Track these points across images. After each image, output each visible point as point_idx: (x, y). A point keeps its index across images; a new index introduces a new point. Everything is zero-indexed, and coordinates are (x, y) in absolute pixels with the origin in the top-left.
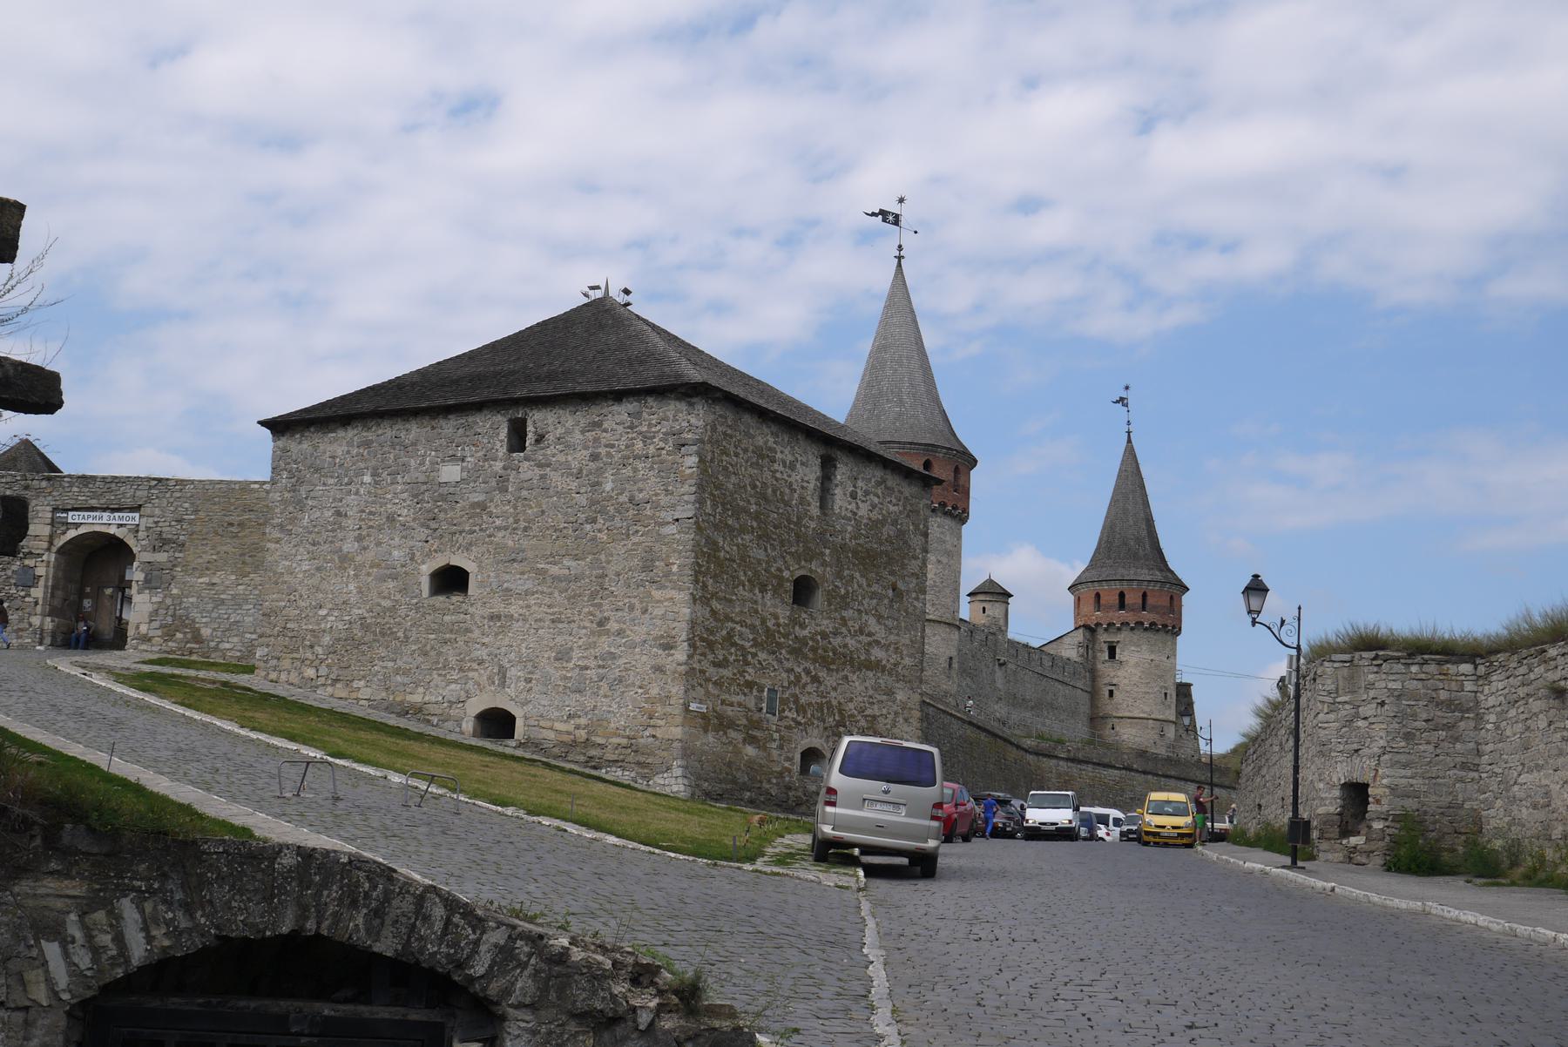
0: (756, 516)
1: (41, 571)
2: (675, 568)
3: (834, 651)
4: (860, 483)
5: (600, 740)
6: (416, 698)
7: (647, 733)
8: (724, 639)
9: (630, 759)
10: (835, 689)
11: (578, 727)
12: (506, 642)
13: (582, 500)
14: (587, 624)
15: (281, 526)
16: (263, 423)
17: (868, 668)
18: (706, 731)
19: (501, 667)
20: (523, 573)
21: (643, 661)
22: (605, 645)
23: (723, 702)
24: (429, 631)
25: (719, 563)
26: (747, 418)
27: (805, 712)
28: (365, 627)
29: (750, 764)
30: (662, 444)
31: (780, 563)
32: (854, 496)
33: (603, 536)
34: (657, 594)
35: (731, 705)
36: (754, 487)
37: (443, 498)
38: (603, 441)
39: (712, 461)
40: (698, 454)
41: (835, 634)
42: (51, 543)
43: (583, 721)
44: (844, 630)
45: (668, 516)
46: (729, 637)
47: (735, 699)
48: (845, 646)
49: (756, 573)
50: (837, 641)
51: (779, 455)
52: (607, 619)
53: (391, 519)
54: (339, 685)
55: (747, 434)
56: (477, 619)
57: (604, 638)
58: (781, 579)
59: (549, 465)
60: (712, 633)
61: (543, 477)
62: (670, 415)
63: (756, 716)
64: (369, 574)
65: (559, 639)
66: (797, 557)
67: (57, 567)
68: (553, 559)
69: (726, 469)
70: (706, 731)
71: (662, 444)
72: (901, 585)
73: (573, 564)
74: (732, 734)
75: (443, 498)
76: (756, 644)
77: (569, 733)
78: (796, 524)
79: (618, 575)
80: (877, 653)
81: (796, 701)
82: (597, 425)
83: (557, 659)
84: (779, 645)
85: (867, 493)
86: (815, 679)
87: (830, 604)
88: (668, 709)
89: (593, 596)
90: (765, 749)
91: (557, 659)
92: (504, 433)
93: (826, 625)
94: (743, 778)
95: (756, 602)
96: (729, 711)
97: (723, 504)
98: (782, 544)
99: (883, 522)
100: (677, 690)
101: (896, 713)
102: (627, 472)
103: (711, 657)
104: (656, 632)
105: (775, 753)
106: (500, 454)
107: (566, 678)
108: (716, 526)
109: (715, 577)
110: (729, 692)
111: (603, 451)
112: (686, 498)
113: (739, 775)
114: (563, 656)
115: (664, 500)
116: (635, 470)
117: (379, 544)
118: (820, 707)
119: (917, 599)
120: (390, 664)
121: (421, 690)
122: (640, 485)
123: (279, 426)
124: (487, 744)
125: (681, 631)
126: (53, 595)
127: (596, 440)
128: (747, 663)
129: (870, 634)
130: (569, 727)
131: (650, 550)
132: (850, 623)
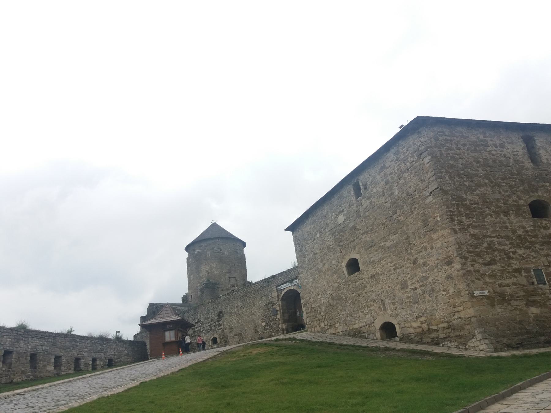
1: (278, 309)
2: (438, 218)
5: (435, 328)
6: (356, 326)
7: (456, 317)
8: (486, 248)
9: (452, 335)
11: (422, 323)
12: (380, 288)
13: (388, 205)
14: (409, 265)
18: (493, 306)
19: (382, 300)
20: (376, 251)
21: (440, 275)
22: (419, 272)
23: (500, 285)
24: (354, 292)
25: (468, 208)
26: (459, 129)
28: (333, 299)
29: (537, 318)
30: (412, 159)
33: (402, 218)
34: (435, 236)
35: (508, 285)
37: (341, 231)
38: (388, 173)
39: (442, 155)
40: (429, 154)
42: (278, 298)
43: (423, 319)
47: (508, 281)
49: (497, 207)
52: (416, 259)
56: (367, 280)
57: (418, 270)
59: (371, 196)
60: (476, 247)
61: (371, 203)
62: (411, 143)
63: (531, 288)
64: (328, 275)
65: (400, 278)
67: (283, 306)
68: (385, 239)
69: (453, 158)
70: (493, 306)
71: (412, 159)
73: (394, 237)
74: (515, 303)
77: (419, 327)
79: (414, 234)
82: (384, 167)
83: (402, 288)
84: (533, 243)
88: (462, 299)
89: (407, 250)
91: (402, 288)
95: (504, 223)
96: (508, 290)
98: (511, 187)
100: (462, 286)
102: (402, 181)
103: (481, 261)
104: (442, 257)
106: (354, 201)
107: (408, 297)
109: (467, 215)
110: (502, 278)
111: (389, 178)
112: (431, 179)
114: (404, 286)
115: (422, 186)
116: (405, 179)
117: (328, 261)
120: (344, 313)
121: (357, 321)
122: (409, 185)
123: (292, 228)
124: (384, 344)
125: (453, 251)
126: (284, 316)
127: (385, 174)
128: (510, 258)
130: (419, 324)
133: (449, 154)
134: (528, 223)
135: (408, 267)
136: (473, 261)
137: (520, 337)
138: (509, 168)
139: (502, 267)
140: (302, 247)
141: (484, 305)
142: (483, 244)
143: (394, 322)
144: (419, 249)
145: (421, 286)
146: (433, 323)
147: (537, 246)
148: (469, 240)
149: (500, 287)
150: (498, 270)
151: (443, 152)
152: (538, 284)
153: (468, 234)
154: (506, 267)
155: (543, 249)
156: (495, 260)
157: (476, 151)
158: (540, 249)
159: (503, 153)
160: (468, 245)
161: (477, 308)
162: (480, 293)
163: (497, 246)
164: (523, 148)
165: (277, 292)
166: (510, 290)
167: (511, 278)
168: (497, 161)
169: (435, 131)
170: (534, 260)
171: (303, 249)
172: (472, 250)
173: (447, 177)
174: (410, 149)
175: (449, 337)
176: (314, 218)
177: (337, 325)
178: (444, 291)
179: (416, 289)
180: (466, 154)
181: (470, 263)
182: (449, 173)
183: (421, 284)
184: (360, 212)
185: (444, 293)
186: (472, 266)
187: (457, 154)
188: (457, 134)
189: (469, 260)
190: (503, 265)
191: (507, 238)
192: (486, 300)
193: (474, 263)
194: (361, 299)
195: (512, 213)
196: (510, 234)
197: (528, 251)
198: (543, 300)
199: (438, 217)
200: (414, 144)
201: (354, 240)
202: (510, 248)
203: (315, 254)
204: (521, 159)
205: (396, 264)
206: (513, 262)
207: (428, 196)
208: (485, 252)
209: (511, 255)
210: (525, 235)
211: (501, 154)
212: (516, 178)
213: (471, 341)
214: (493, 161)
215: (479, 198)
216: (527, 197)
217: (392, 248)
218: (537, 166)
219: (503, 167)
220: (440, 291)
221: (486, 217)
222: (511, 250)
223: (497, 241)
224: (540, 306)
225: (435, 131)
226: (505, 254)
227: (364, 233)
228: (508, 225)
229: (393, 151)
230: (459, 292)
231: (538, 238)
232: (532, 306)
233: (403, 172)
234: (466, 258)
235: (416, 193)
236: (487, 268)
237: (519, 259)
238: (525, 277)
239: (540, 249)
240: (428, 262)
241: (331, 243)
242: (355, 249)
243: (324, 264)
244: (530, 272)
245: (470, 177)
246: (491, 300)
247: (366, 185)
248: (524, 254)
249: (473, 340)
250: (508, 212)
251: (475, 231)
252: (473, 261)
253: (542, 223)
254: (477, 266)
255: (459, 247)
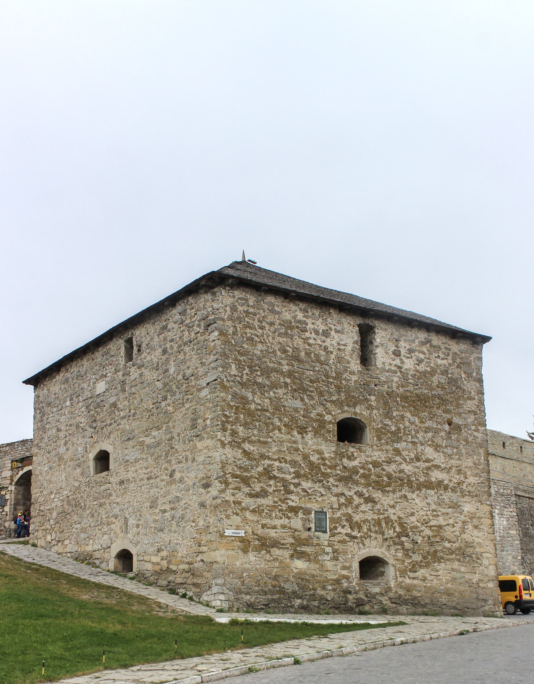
0: (290, 374)
1: (7, 497)
2: (208, 422)
3: (389, 476)
4: (402, 344)
5: (174, 568)
6: (89, 548)
7: (199, 559)
8: (260, 474)
10: (393, 507)
12: (127, 500)
13: (159, 385)
14: (165, 477)
15: (37, 445)
16: (27, 382)
17: (428, 487)
18: (245, 551)
20: (133, 447)
21: (193, 499)
24: (96, 499)
25: (250, 414)
26: (270, 299)
27: (360, 527)
28: (69, 503)
29: (301, 576)
30: (198, 329)
31: (320, 409)
32: (397, 354)
33: (170, 408)
34: (199, 445)
35: (274, 527)
36: (285, 351)
39: (234, 333)
41: (389, 462)
42: (12, 480)
43: (164, 553)
44: (398, 458)
45: (203, 382)
46: (267, 473)
47: (278, 522)
48: (401, 471)
49: (293, 419)
50: (391, 468)
51: (310, 326)
53: (78, 427)
54: (60, 544)
55: (273, 311)
56: (114, 485)
57: (173, 486)
58: (322, 423)
60: (246, 470)
61: (141, 375)
62: (201, 305)
63: (305, 535)
64: (69, 466)
66: (339, 404)
67: (17, 494)
68: (147, 432)
70: (245, 551)
71: (198, 329)
72: (456, 420)
73: (155, 433)
74: (276, 552)
75: (98, 406)
76: (298, 475)
77: (158, 564)
78: (334, 378)
80: (436, 475)
81: (349, 519)
82: (165, 328)
84: (326, 476)
85: (411, 351)
86: (369, 500)
87: (379, 439)
88: (209, 537)
90: (317, 561)
92: (123, 350)
93: (378, 455)
94: (289, 587)
95: (295, 442)
96: (272, 533)
97: (250, 367)
98: (321, 394)
99: (433, 372)
101: (464, 522)
102: (181, 357)
103: (247, 490)
105: (329, 565)
107: (155, 521)
108: (243, 385)
109: (245, 425)
111: (168, 346)
112: (212, 365)
113: (287, 586)
115: (201, 371)
118: (378, 523)
119: (477, 430)
120: (79, 526)
121: (91, 541)
127: (165, 339)
129: (428, 461)
131: (195, 412)
132: (404, 453)
133: (246, 333)
134: (329, 448)
135: (163, 480)
136: (236, 488)
137: (269, 597)
138: (327, 368)
139: (275, 502)
140: (44, 415)
141: (233, 550)
142: (257, 467)
143: (133, 551)
144: (180, 457)
145: (172, 509)
146: (173, 561)
147: (331, 480)
148: (239, 460)
149: (263, 528)
150: (267, 506)
151: (238, 329)
152: (316, 531)
153: (240, 451)
154: (280, 503)
155: (337, 486)
156: (268, 492)
157: (286, 334)
158: (334, 485)
159: (324, 344)
160: (236, 466)
161: (223, 552)
162: (233, 533)
163: (275, 473)
164: (355, 342)
165: (12, 469)
166: (275, 535)
167: (281, 518)
168: (313, 355)
169: (234, 297)
170: (320, 499)
171: (45, 418)
172: (238, 473)
173: (233, 366)
174: (198, 312)
175: (185, 583)
176: (68, 375)
177: (67, 542)
178: (193, 522)
179: (165, 511)
180: (270, 338)
181: (231, 491)
182: (240, 361)
183: (172, 506)
184: (125, 384)
185: (193, 524)
186: (233, 495)
187: (257, 336)
188: (266, 307)
189: (230, 487)
190: (276, 499)
191: (293, 463)
192: (238, 543)
193: (237, 491)
194: (101, 511)
195: (310, 431)
196: (299, 458)
197: (317, 486)
198: (316, 553)
199: (209, 420)
200: (205, 308)
201: (111, 424)
202: (293, 478)
203: (59, 430)
204: (346, 357)
205: (151, 472)
206: (291, 497)
207: (204, 388)
208: (256, 478)
209: (292, 487)
210: (319, 464)
211: (321, 346)
212: (332, 383)
213: (205, 594)
214: (306, 353)
215: (271, 403)
216: (340, 411)
217: (151, 448)
218: (368, 370)
219: (318, 364)
220: (189, 520)
221: (273, 430)
222: (293, 481)
223: (277, 467)
224: (309, 560)
225: (234, 297)
226: (284, 486)
227: (123, 418)
228: (300, 447)
229: (179, 308)
230: (208, 527)
231: (336, 470)
232: (298, 559)
233: (185, 344)
234: (227, 483)
235: (193, 378)
236: (252, 500)
237: (301, 495)
238: (302, 519)
239: (334, 485)
240: (186, 479)
241: (83, 420)
242: (109, 437)
243: (68, 449)
244: (310, 513)
245: (266, 372)
246: (245, 545)
247: (140, 346)
248: (310, 488)
249: (208, 593)
250: (305, 428)
251: (252, 448)
252: (236, 488)
253: (348, 451)
254: (240, 496)
255: (223, 467)
